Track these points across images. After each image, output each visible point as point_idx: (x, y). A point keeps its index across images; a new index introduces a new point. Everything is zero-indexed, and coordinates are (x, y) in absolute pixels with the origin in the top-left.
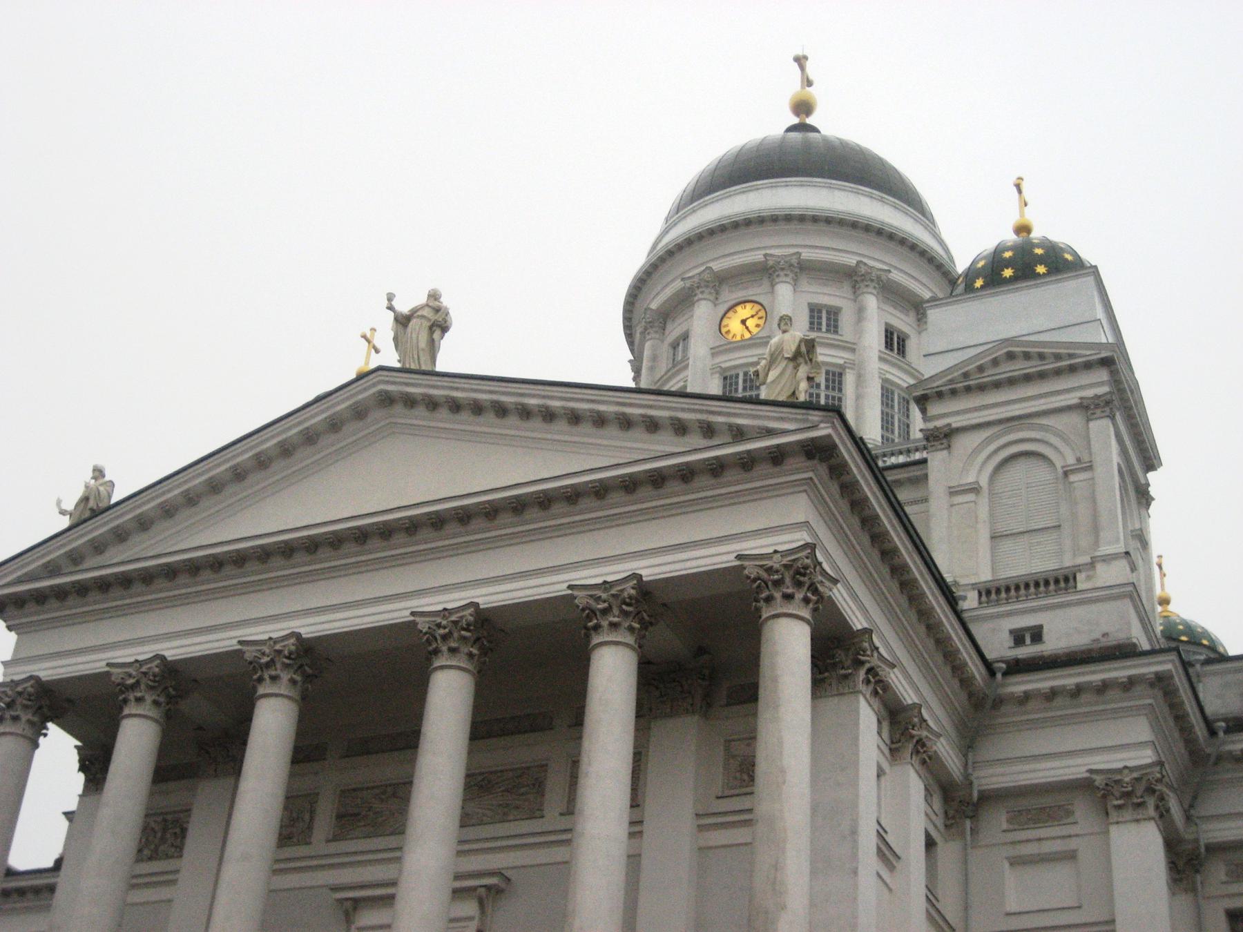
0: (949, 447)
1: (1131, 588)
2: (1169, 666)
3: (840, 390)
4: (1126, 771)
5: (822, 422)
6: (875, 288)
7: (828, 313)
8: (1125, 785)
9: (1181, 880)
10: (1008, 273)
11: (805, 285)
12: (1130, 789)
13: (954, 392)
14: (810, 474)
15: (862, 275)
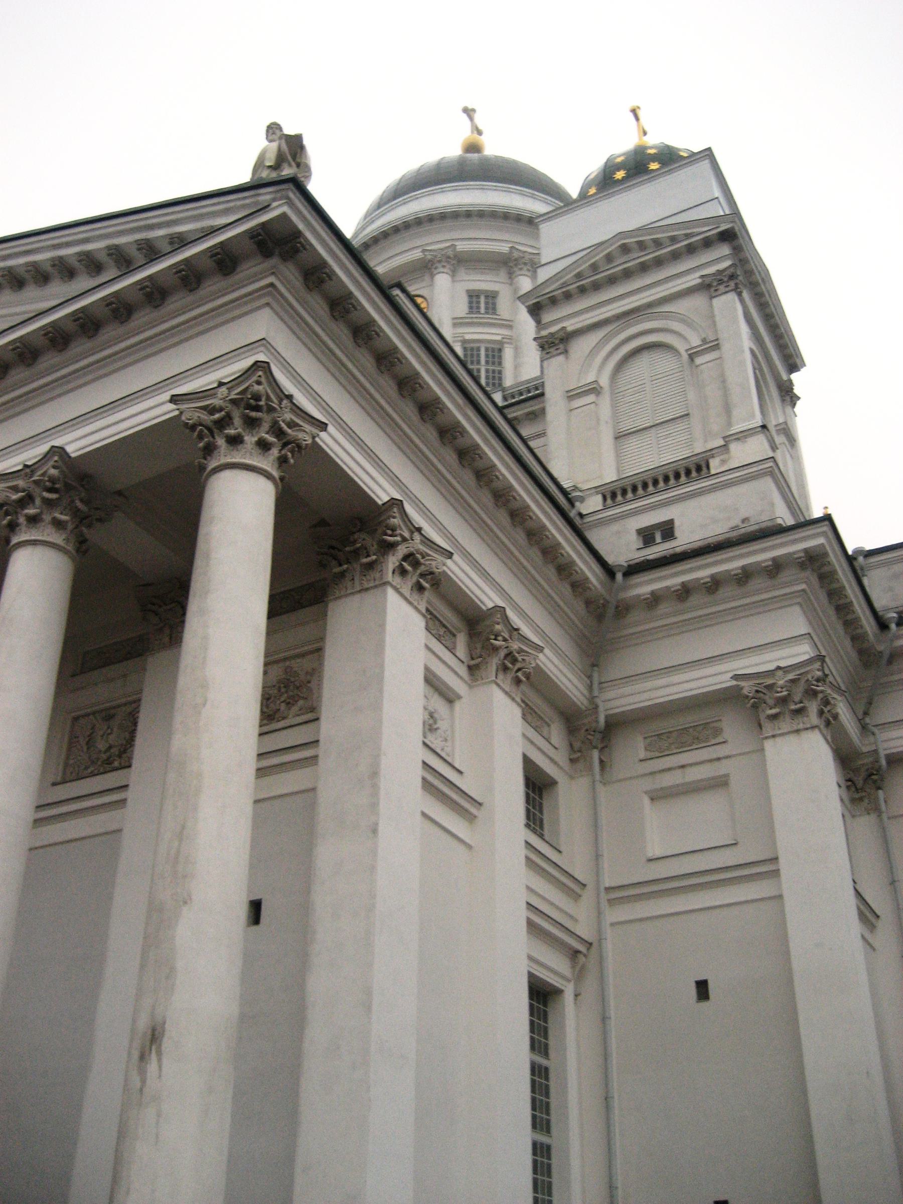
0: (566, 352)
1: (771, 464)
2: (821, 540)
3: (500, 364)
4: (780, 673)
5: (274, 200)
6: (528, 270)
7: (487, 297)
8: (779, 689)
9: (861, 799)
10: (620, 175)
11: (462, 274)
12: (785, 693)
13: (568, 296)
14: (271, 279)
15: (516, 260)
